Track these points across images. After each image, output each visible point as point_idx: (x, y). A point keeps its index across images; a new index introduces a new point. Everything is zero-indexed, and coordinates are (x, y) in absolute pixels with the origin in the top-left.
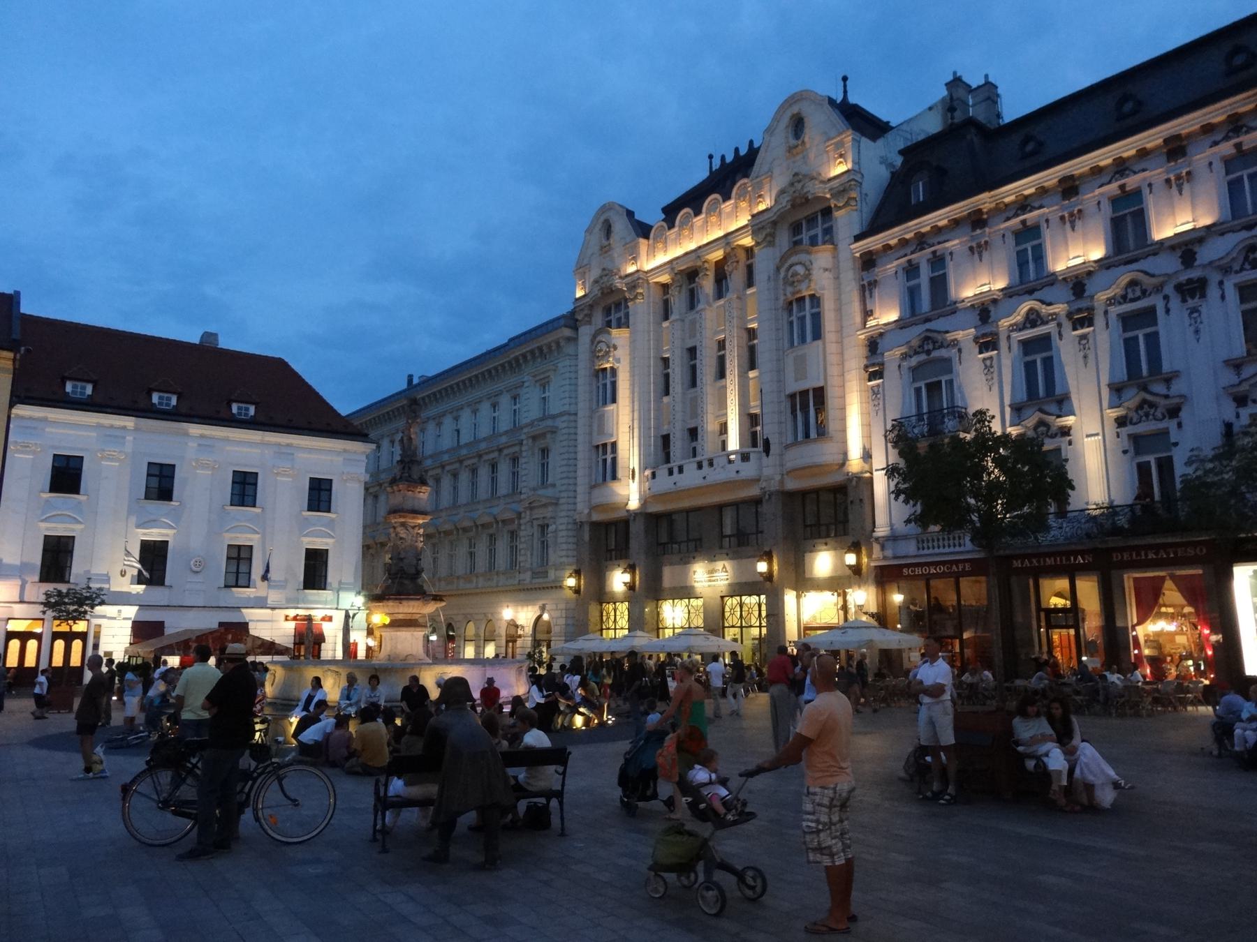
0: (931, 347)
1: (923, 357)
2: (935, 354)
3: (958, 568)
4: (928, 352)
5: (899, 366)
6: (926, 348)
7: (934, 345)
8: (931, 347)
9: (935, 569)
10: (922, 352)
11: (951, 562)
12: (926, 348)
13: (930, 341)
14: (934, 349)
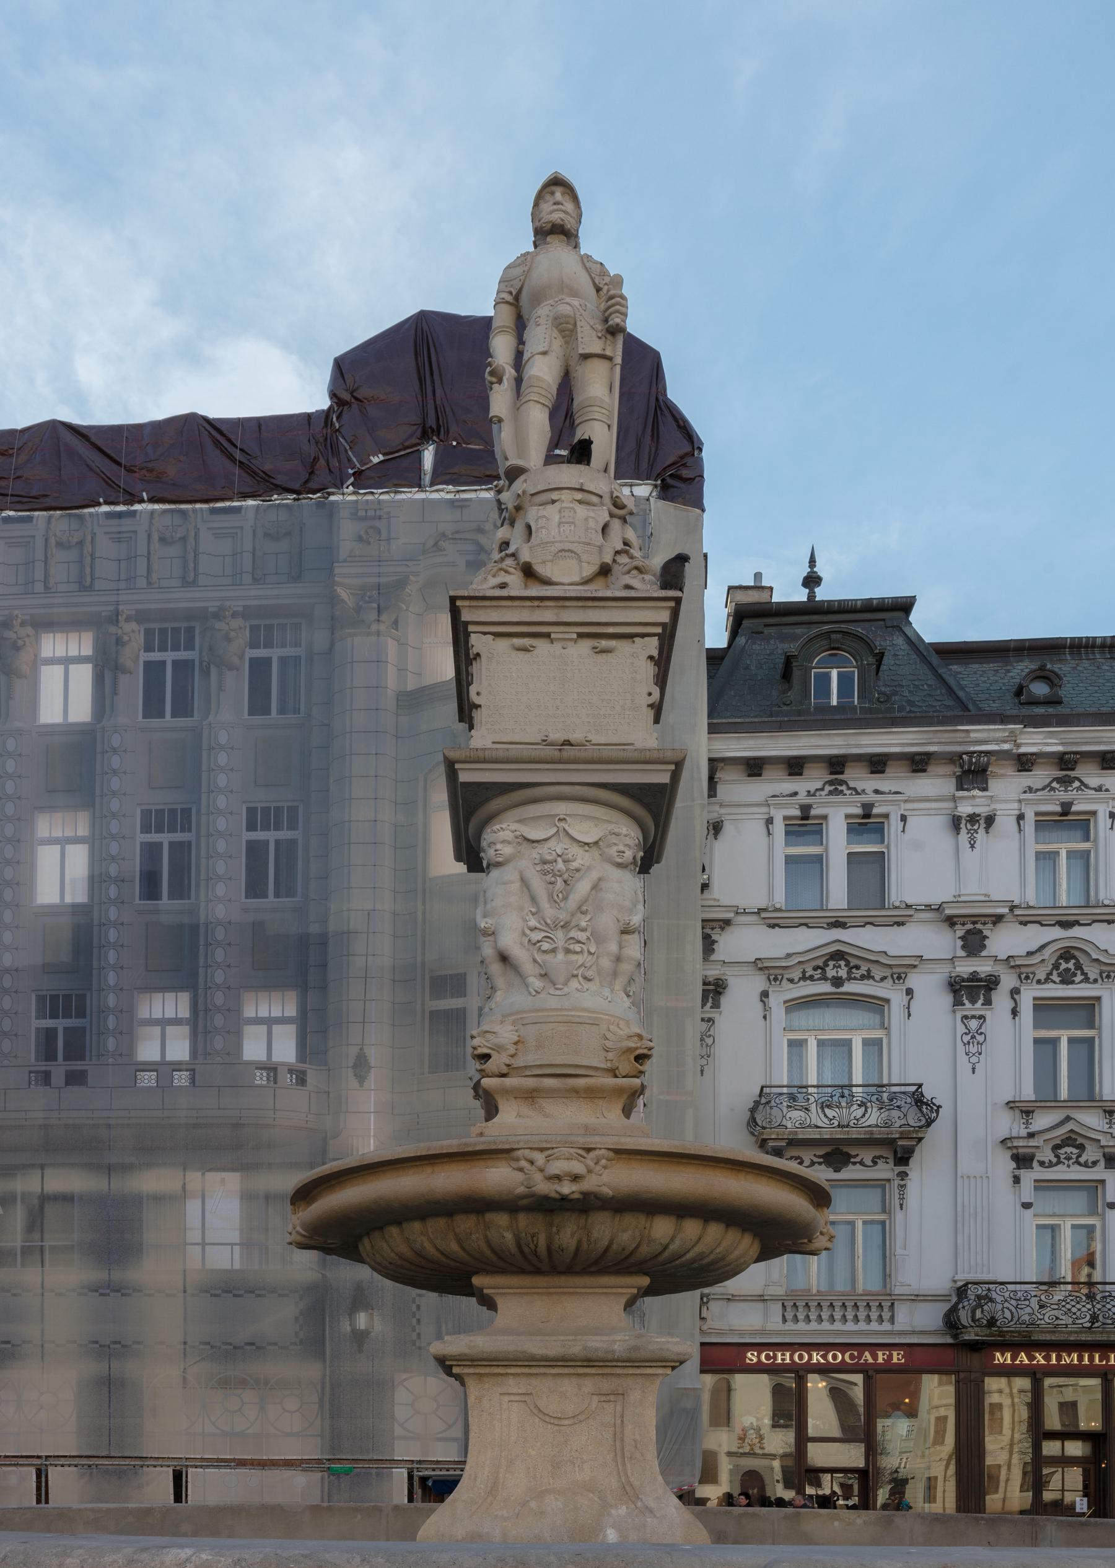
0: (843, 973)
1: (826, 987)
2: (849, 987)
3: (875, 1357)
4: (837, 982)
5: (765, 994)
6: (831, 973)
7: (849, 972)
8: (843, 973)
9: (824, 1357)
10: (825, 978)
11: (861, 1347)
12: (831, 973)
13: (842, 963)
14: (849, 979)
